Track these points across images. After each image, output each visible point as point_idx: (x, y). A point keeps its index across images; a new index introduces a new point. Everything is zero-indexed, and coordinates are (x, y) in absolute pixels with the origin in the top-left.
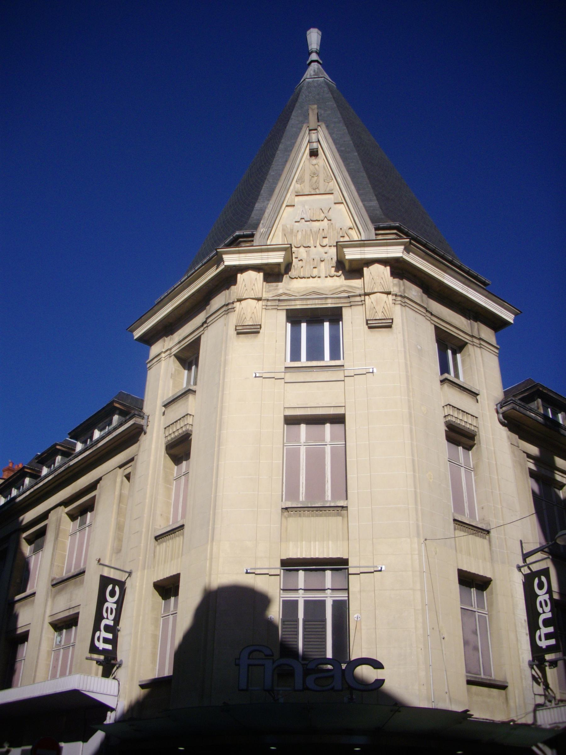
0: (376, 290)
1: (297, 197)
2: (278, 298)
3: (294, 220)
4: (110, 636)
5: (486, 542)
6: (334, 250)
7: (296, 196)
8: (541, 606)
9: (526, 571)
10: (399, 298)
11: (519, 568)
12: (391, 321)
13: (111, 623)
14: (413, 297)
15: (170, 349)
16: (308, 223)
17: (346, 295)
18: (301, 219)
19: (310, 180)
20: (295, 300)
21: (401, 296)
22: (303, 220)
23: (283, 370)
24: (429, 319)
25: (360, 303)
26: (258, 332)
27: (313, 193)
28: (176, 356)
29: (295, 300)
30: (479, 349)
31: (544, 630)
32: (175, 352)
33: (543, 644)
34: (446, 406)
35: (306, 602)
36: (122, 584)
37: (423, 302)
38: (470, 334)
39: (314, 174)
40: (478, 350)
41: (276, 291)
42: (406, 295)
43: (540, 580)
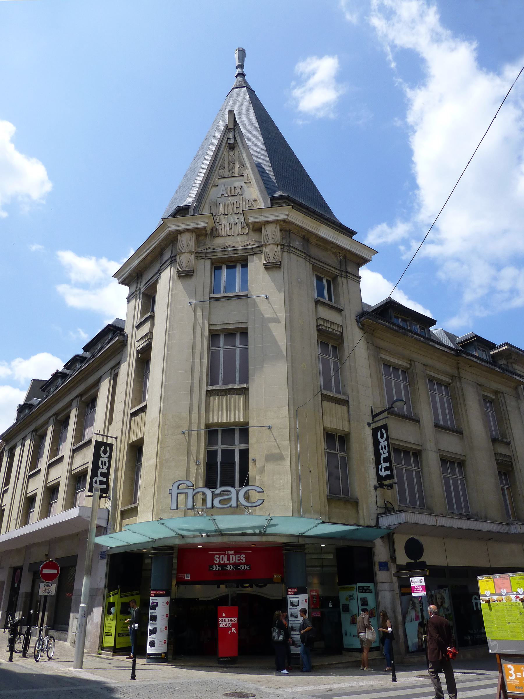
0: (269, 243)
1: (220, 180)
4: (104, 479)
5: (345, 408)
6: (242, 217)
8: (382, 449)
9: (374, 426)
10: (286, 248)
11: (369, 424)
13: (106, 471)
15: (140, 289)
17: (250, 247)
20: (216, 252)
21: (287, 246)
26: (192, 275)
27: (230, 176)
29: (216, 252)
30: (345, 279)
31: (384, 465)
33: (383, 474)
35: (223, 451)
36: (111, 446)
39: (232, 162)
40: (344, 280)
43: (381, 432)
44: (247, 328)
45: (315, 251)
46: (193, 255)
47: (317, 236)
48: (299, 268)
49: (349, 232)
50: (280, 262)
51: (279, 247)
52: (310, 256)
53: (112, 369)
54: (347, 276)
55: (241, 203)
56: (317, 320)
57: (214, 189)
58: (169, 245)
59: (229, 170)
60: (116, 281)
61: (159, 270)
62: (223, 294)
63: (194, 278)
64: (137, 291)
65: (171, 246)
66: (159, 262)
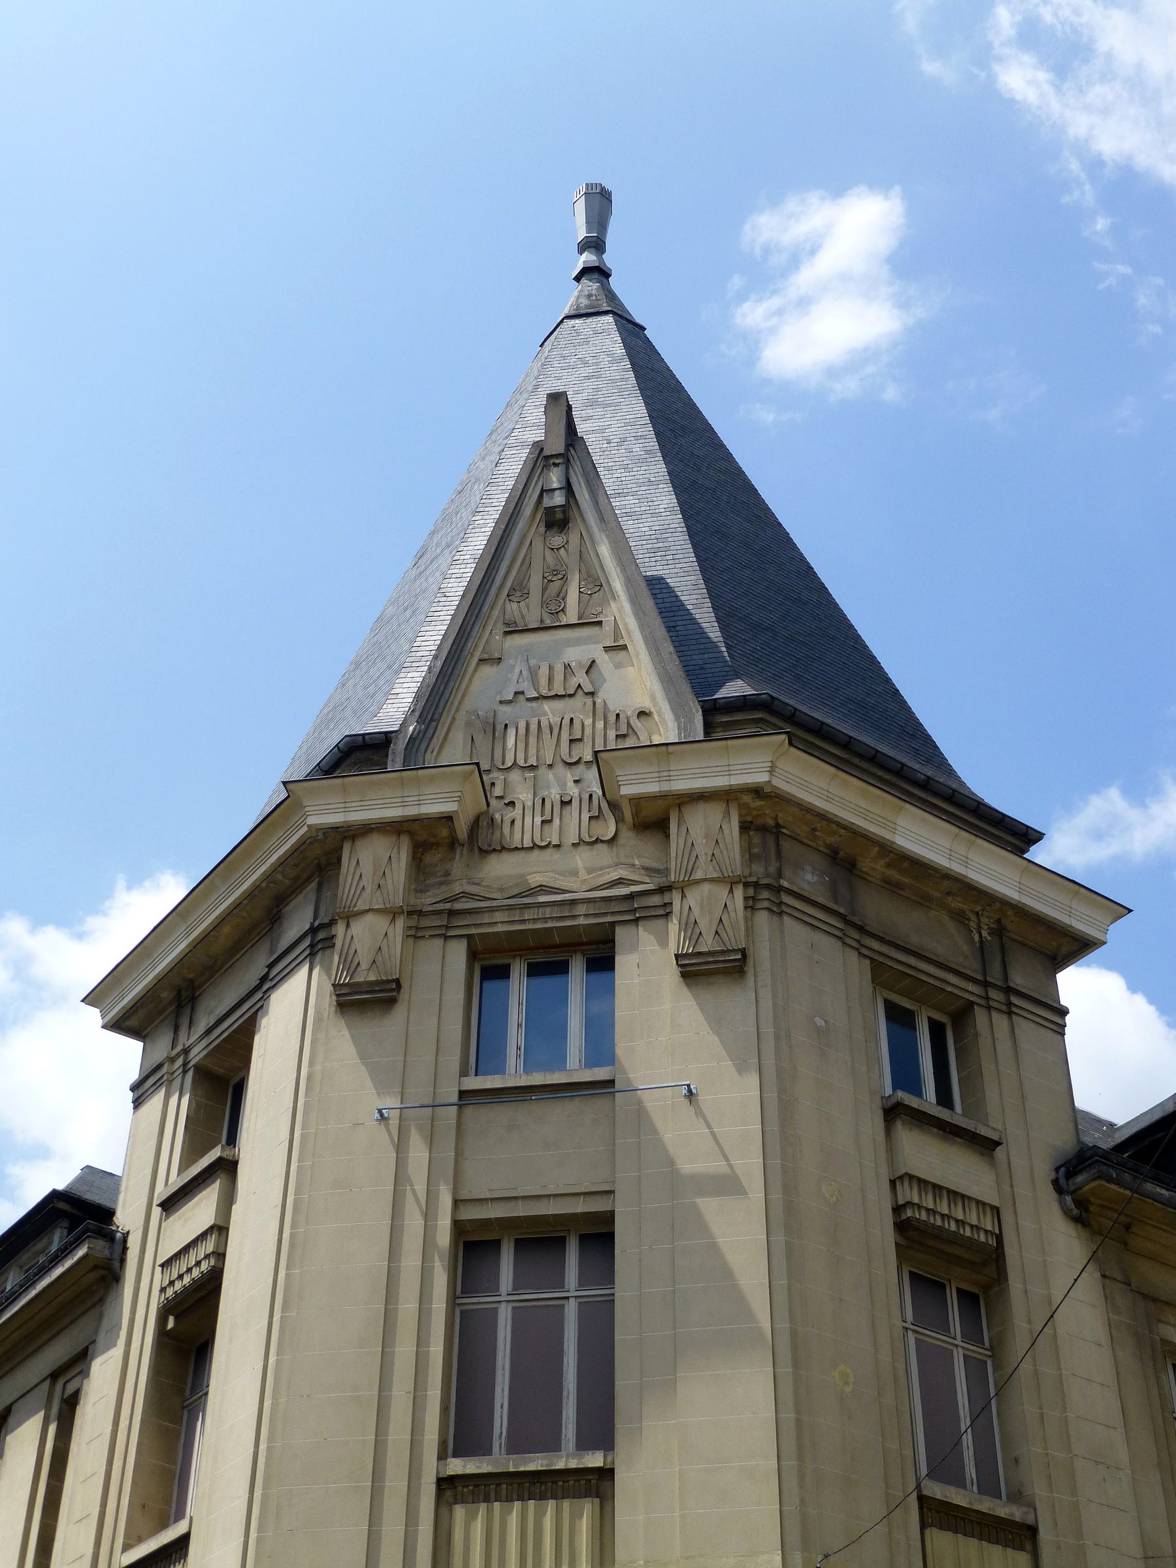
0: (698, 875)
1: (509, 637)
2: (448, 906)
3: (498, 698)
6: (592, 775)
7: (507, 633)
10: (765, 894)
12: (739, 956)
14: (806, 886)
16: (534, 704)
17: (623, 891)
18: (516, 693)
19: (544, 590)
20: (491, 910)
21: (768, 887)
22: (521, 697)
23: (455, 1098)
24: (854, 944)
25: (662, 912)
26: (392, 1001)
27: (548, 622)
28: (198, 1068)
29: (491, 910)
30: (1005, 1017)
32: (198, 1058)
34: (901, 1178)
37: (836, 902)
38: (979, 977)
39: (555, 572)
40: (1001, 1022)
41: (444, 888)
42: (785, 884)
44: (608, 1218)
45: (878, 909)
46: (400, 923)
47: (886, 849)
48: (818, 976)
49: (1014, 834)
50: (743, 952)
51: (739, 893)
52: (861, 929)
53: (54, 1376)
54: (1009, 1004)
55: (588, 722)
56: (893, 1183)
57: (488, 671)
58: (308, 880)
59: (544, 604)
60: (94, 1015)
61: (264, 979)
62: (514, 1075)
63: (399, 1011)
64: (172, 1060)
65: (314, 885)
66: (265, 945)
